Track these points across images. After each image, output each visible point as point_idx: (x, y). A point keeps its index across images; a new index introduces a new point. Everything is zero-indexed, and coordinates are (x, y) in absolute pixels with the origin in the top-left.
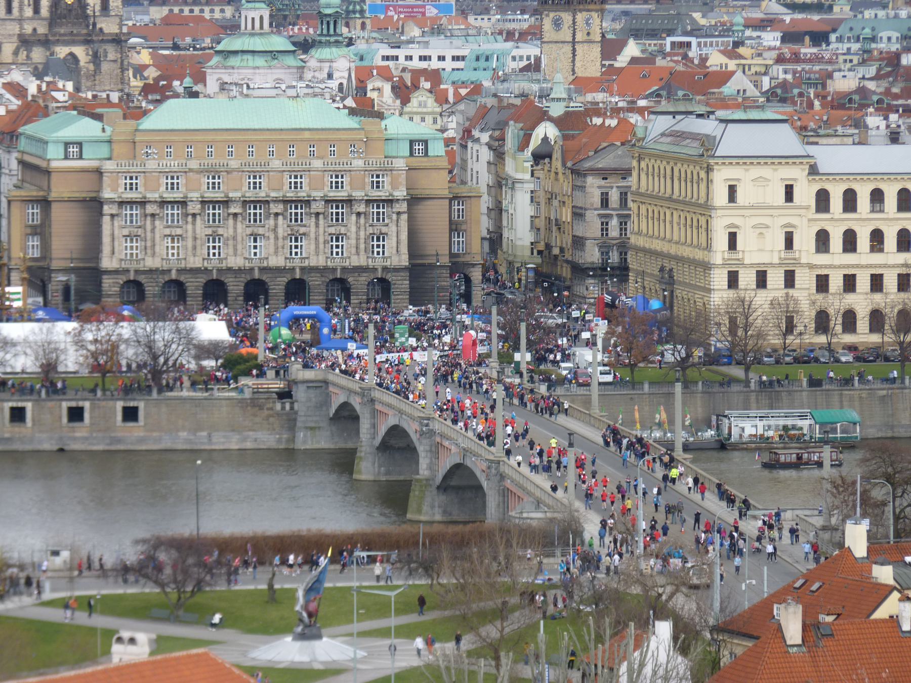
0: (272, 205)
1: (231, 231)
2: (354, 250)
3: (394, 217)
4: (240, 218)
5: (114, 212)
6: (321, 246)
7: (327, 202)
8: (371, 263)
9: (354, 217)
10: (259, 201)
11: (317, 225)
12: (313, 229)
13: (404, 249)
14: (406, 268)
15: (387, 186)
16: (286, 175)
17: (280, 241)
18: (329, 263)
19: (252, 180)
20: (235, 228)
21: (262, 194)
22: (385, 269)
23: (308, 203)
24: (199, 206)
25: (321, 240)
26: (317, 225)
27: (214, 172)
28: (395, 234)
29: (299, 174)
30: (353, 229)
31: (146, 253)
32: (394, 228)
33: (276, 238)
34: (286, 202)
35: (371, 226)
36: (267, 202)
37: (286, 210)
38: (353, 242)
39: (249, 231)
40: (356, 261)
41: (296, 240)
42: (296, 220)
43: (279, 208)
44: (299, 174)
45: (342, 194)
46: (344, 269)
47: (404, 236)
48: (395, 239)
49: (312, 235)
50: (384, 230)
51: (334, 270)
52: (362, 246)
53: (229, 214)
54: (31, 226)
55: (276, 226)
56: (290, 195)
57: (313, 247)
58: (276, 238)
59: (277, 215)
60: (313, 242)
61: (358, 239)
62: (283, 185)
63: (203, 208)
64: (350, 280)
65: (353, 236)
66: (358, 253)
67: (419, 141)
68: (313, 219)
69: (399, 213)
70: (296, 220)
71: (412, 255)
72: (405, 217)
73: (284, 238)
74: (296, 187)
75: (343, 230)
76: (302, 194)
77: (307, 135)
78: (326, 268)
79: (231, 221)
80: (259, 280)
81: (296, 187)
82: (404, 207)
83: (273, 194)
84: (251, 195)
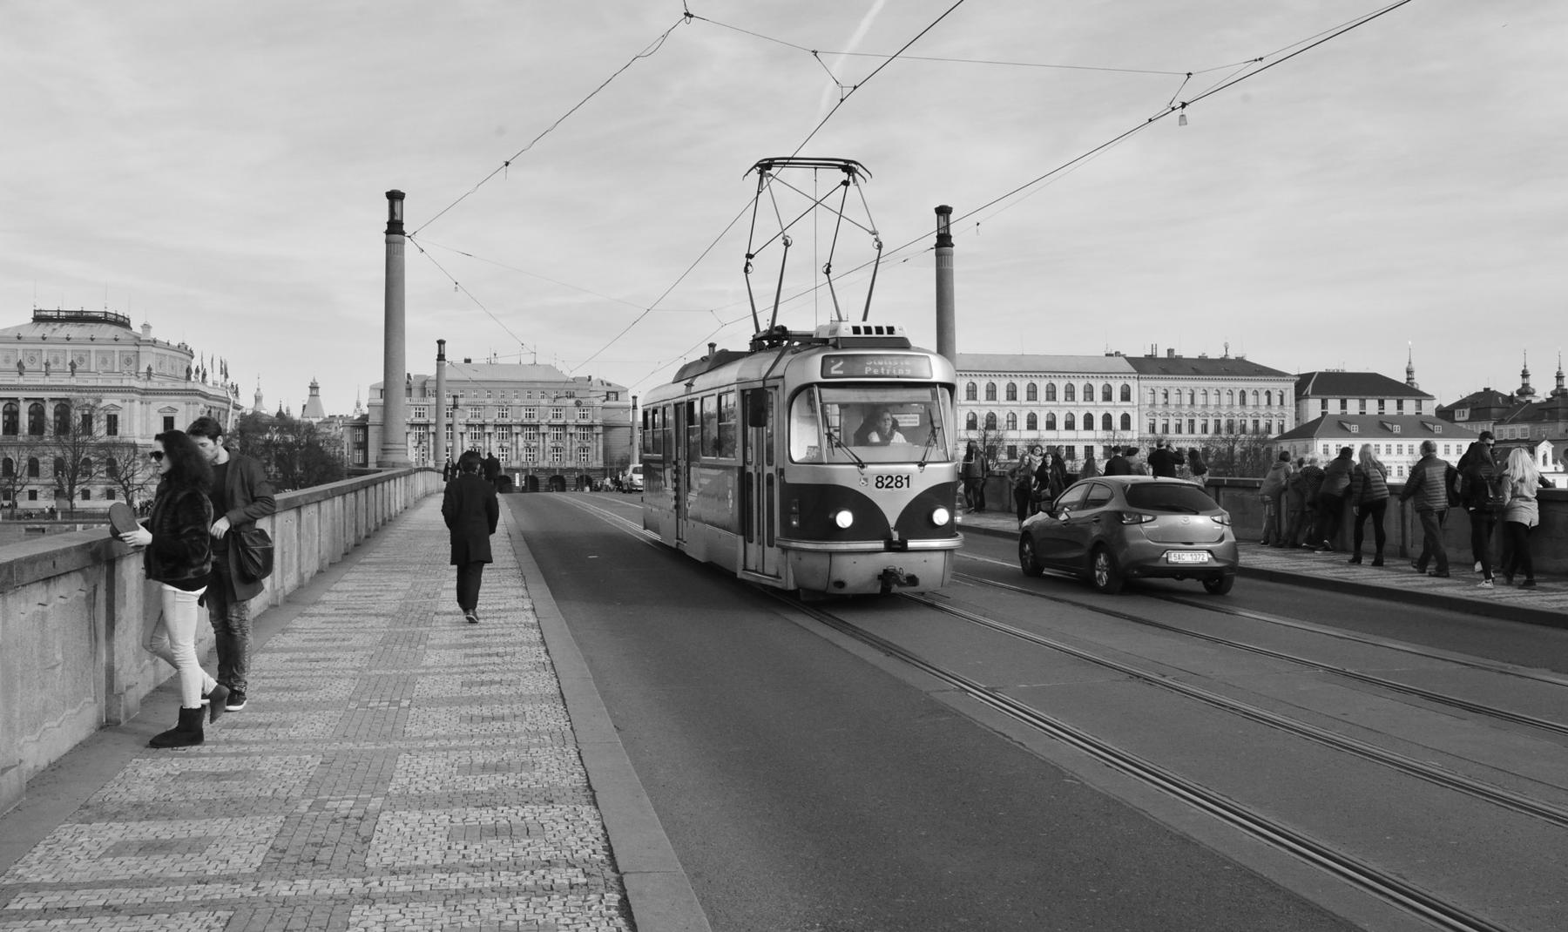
0: (513, 427)
1: (487, 444)
2: (568, 458)
3: (595, 436)
4: (492, 436)
5: (407, 431)
6: (547, 454)
7: (550, 426)
8: (579, 466)
9: (568, 436)
10: (505, 425)
11: (544, 442)
12: (541, 444)
13: (601, 457)
14: (602, 469)
15: (590, 417)
16: (523, 409)
17: (520, 452)
18: (551, 466)
19: (501, 412)
20: (490, 442)
21: (507, 421)
22: (588, 469)
23: (537, 427)
24: (465, 428)
25: (547, 451)
26: (544, 442)
27: (476, 407)
28: (595, 447)
29: (532, 408)
30: (568, 444)
31: (429, 458)
32: (595, 444)
33: (517, 449)
34: (523, 426)
35: (579, 442)
36: (511, 426)
37: (523, 431)
38: (568, 452)
39: (499, 445)
40: (569, 464)
41: (530, 451)
42: (530, 438)
43: (518, 429)
44: (532, 408)
45: (560, 422)
46: (561, 469)
47: (601, 449)
48: (595, 450)
49: (541, 448)
50: (587, 445)
51: (554, 470)
52: (574, 455)
53: (485, 434)
54: (357, 443)
55: (517, 441)
56: (526, 421)
57: (541, 455)
58: (517, 449)
59: (517, 434)
60: (541, 451)
61: (571, 450)
62: (521, 414)
63: (468, 429)
64: (565, 476)
65: (568, 448)
66: (571, 459)
67: (613, 392)
68: (541, 437)
69: (597, 434)
70: (530, 438)
71: (605, 462)
72: (601, 436)
73: (523, 449)
74: (530, 417)
75: (560, 445)
76: (534, 421)
77: (539, 385)
78: (549, 469)
79: (487, 438)
80: (505, 476)
81: (530, 417)
82: (600, 430)
83: (514, 421)
84: (500, 421)
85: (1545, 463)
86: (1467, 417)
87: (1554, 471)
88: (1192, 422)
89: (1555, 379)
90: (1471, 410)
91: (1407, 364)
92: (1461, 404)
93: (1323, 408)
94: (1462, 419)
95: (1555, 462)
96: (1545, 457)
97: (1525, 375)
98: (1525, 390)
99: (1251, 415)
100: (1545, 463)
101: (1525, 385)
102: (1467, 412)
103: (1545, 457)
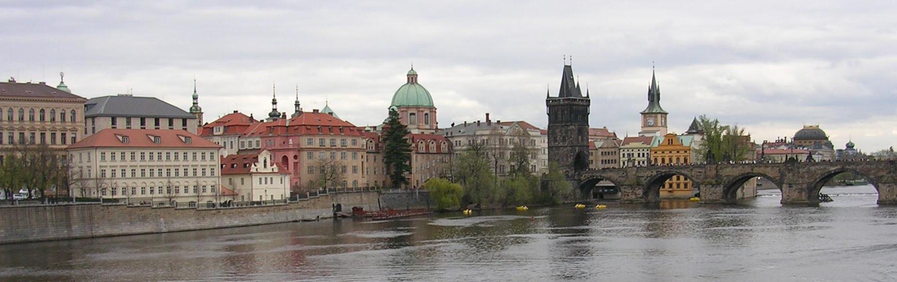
85: (265, 166)
86: (221, 132)
87: (271, 171)
88: (64, 135)
89: (295, 106)
90: (225, 127)
91: (193, 93)
92: (218, 123)
93: (113, 124)
94: (218, 133)
95: (272, 165)
96: (265, 162)
97: (274, 102)
98: (274, 115)
99: (39, 129)
100: (265, 166)
101: (275, 110)
102: (222, 129)
103: (265, 162)
